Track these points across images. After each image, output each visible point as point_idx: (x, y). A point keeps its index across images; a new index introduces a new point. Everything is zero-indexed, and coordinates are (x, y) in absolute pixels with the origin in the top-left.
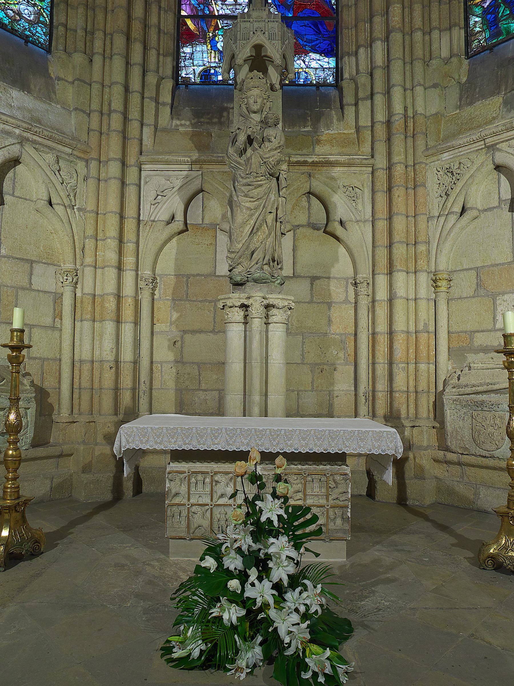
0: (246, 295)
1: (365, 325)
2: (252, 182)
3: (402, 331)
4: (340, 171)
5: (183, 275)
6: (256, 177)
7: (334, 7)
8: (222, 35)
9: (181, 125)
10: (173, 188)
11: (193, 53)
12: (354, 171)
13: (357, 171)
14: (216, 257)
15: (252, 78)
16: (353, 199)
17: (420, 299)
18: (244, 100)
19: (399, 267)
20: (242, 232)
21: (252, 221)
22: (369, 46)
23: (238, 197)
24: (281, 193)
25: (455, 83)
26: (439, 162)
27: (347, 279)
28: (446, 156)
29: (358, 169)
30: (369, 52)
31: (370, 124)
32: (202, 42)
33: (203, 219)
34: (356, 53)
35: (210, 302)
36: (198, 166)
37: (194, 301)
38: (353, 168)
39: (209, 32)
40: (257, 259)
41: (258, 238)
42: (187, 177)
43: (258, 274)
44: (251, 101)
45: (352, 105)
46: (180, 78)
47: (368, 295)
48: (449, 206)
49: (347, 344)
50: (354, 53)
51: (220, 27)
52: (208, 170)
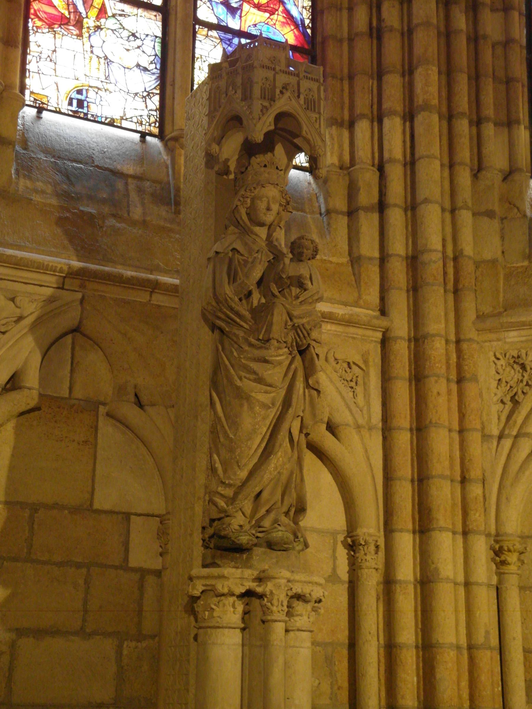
0: (256, 573)
1: (374, 627)
2: (271, 356)
3: (451, 646)
4: (330, 330)
5: (23, 505)
6: (279, 348)
7: (309, 31)
8: (112, 30)
9: (36, 191)
10: (20, 318)
11: (55, 51)
12: (354, 334)
13: (357, 334)
14: (94, 470)
15: (265, 166)
16: (353, 384)
17: (477, 584)
18: (246, 199)
19: (442, 523)
20: (250, 448)
21: (265, 429)
22: (376, 119)
23: (241, 379)
24: (310, 382)
25: (520, 216)
26: (500, 343)
27: (334, 534)
28: (513, 336)
29: (360, 331)
30: (376, 130)
31: (377, 254)
32: (75, 33)
33: (71, 389)
34: (351, 125)
35: (78, 566)
36: (77, 282)
37: (45, 563)
38: (352, 330)
39: (87, 17)
40: (272, 503)
41: (277, 462)
42: (51, 300)
43: (280, 533)
44: (262, 206)
45: (342, 213)
46: (27, 92)
47: (377, 569)
48: (520, 421)
49: (335, 664)
50: (346, 123)
51: (110, 14)
52: (96, 293)
